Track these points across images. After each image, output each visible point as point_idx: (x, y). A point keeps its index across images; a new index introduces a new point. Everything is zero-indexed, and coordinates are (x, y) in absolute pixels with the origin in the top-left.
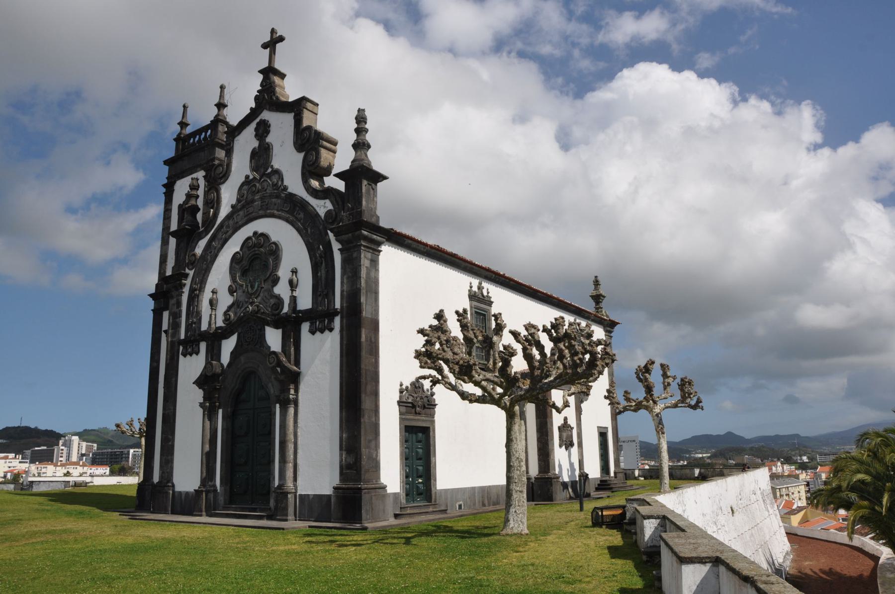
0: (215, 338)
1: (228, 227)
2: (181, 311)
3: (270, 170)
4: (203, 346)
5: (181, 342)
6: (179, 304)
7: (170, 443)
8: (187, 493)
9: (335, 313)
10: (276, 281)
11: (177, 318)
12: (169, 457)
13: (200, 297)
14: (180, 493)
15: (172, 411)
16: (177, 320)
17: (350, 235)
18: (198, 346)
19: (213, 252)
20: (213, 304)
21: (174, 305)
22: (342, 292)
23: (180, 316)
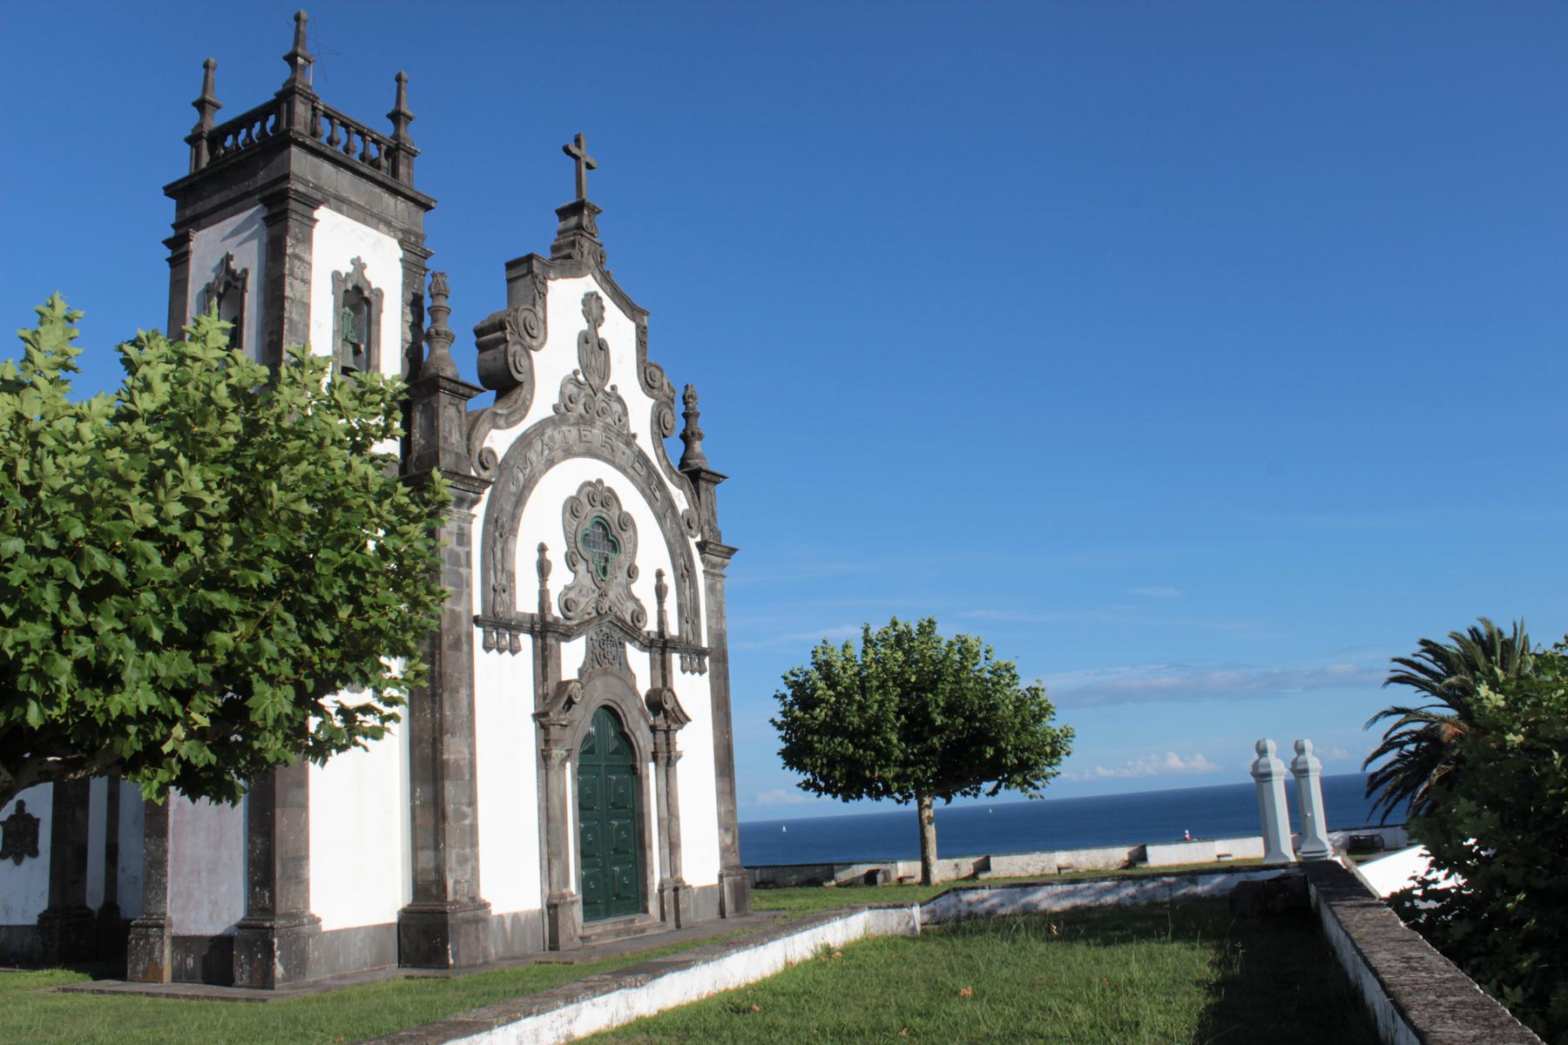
0: (546, 632)
1: (551, 438)
2: (468, 554)
3: (608, 389)
4: (526, 640)
5: (476, 620)
6: (463, 538)
7: (467, 822)
8: (516, 917)
9: (701, 653)
10: (632, 573)
11: (460, 566)
12: (468, 850)
13: (511, 545)
14: (501, 917)
15: (468, 756)
16: (463, 571)
17: (720, 559)
18: (514, 637)
19: (528, 470)
20: (543, 569)
21: (450, 533)
22: (709, 628)
23: (469, 565)
